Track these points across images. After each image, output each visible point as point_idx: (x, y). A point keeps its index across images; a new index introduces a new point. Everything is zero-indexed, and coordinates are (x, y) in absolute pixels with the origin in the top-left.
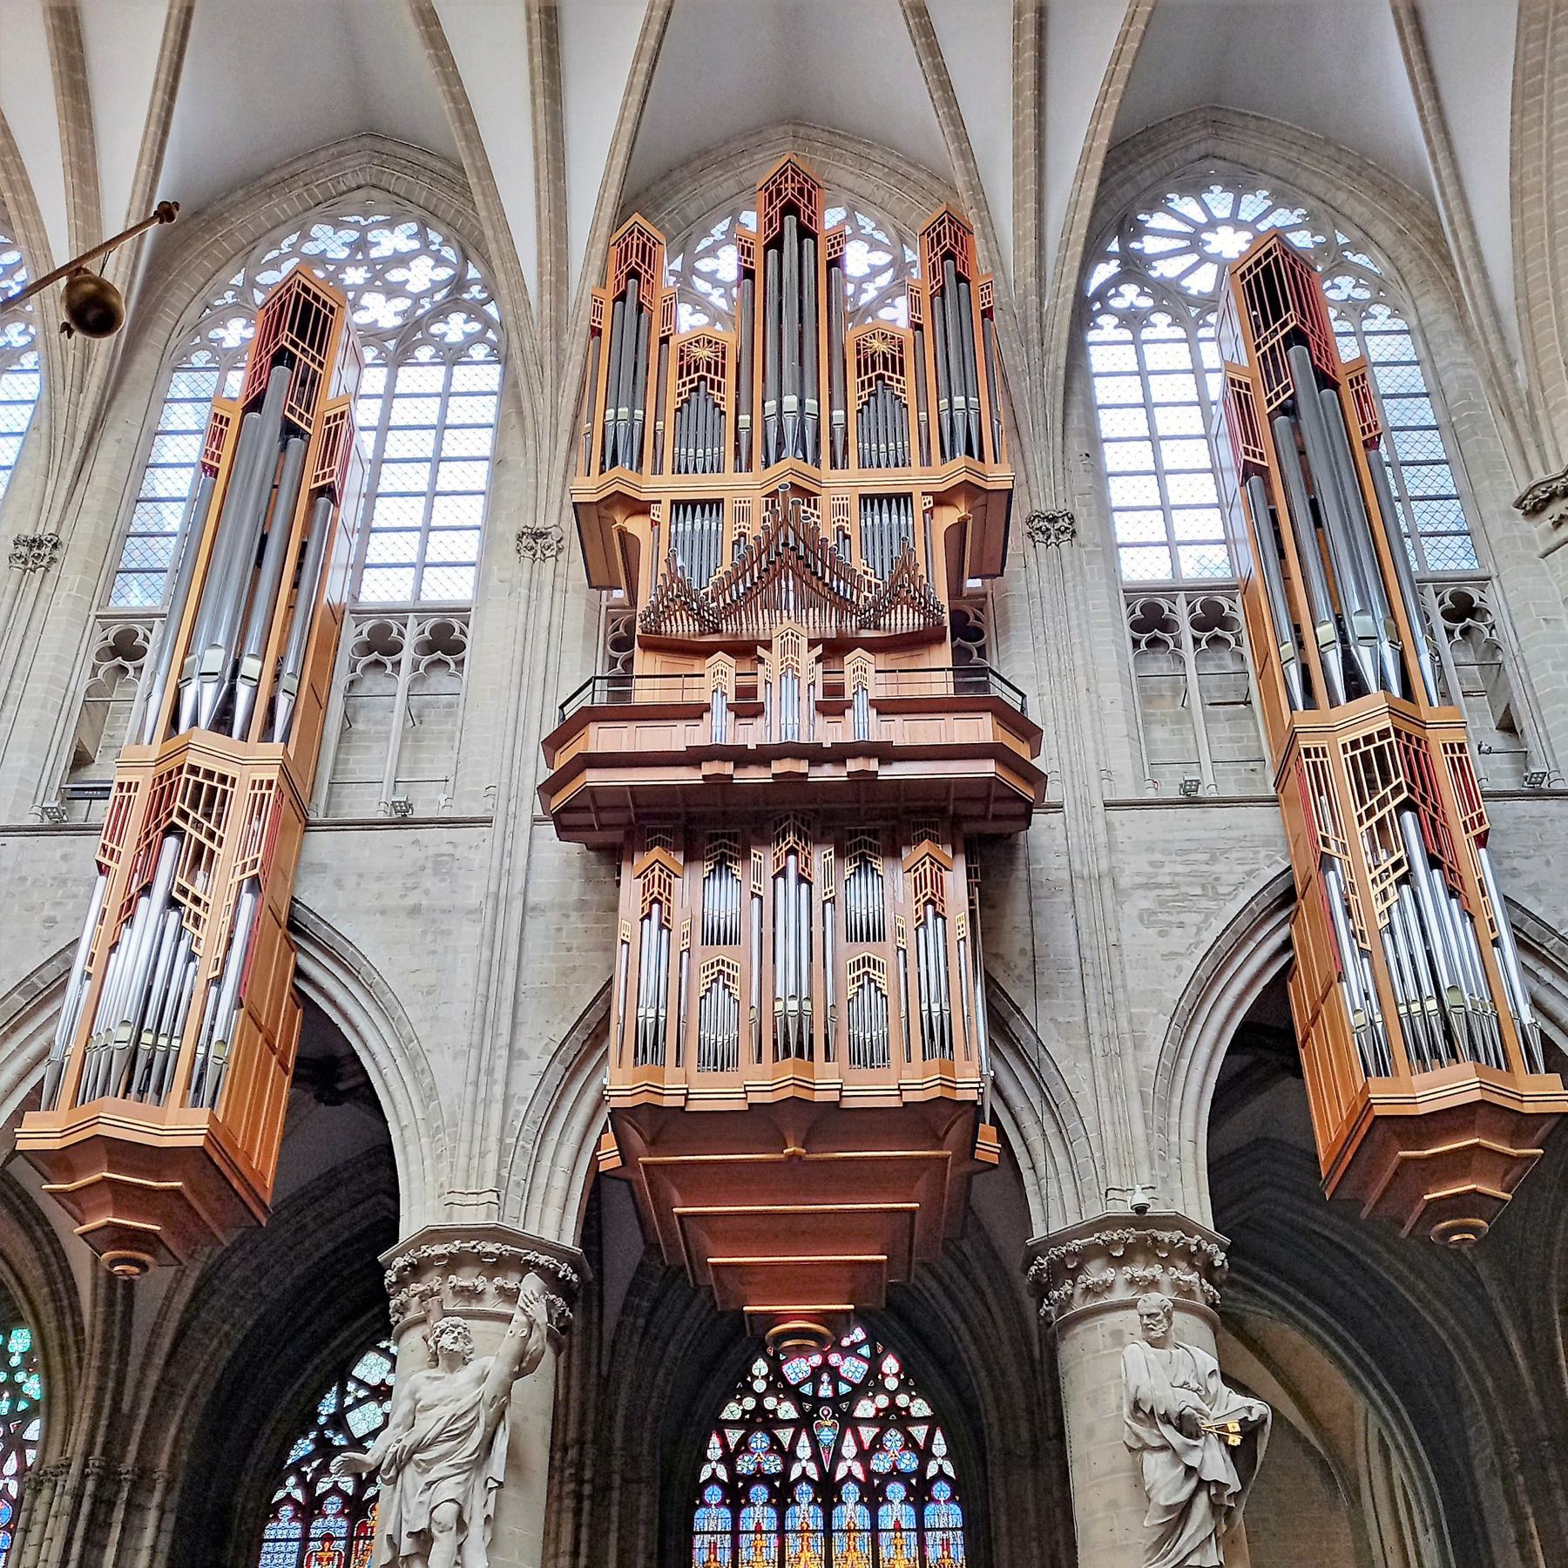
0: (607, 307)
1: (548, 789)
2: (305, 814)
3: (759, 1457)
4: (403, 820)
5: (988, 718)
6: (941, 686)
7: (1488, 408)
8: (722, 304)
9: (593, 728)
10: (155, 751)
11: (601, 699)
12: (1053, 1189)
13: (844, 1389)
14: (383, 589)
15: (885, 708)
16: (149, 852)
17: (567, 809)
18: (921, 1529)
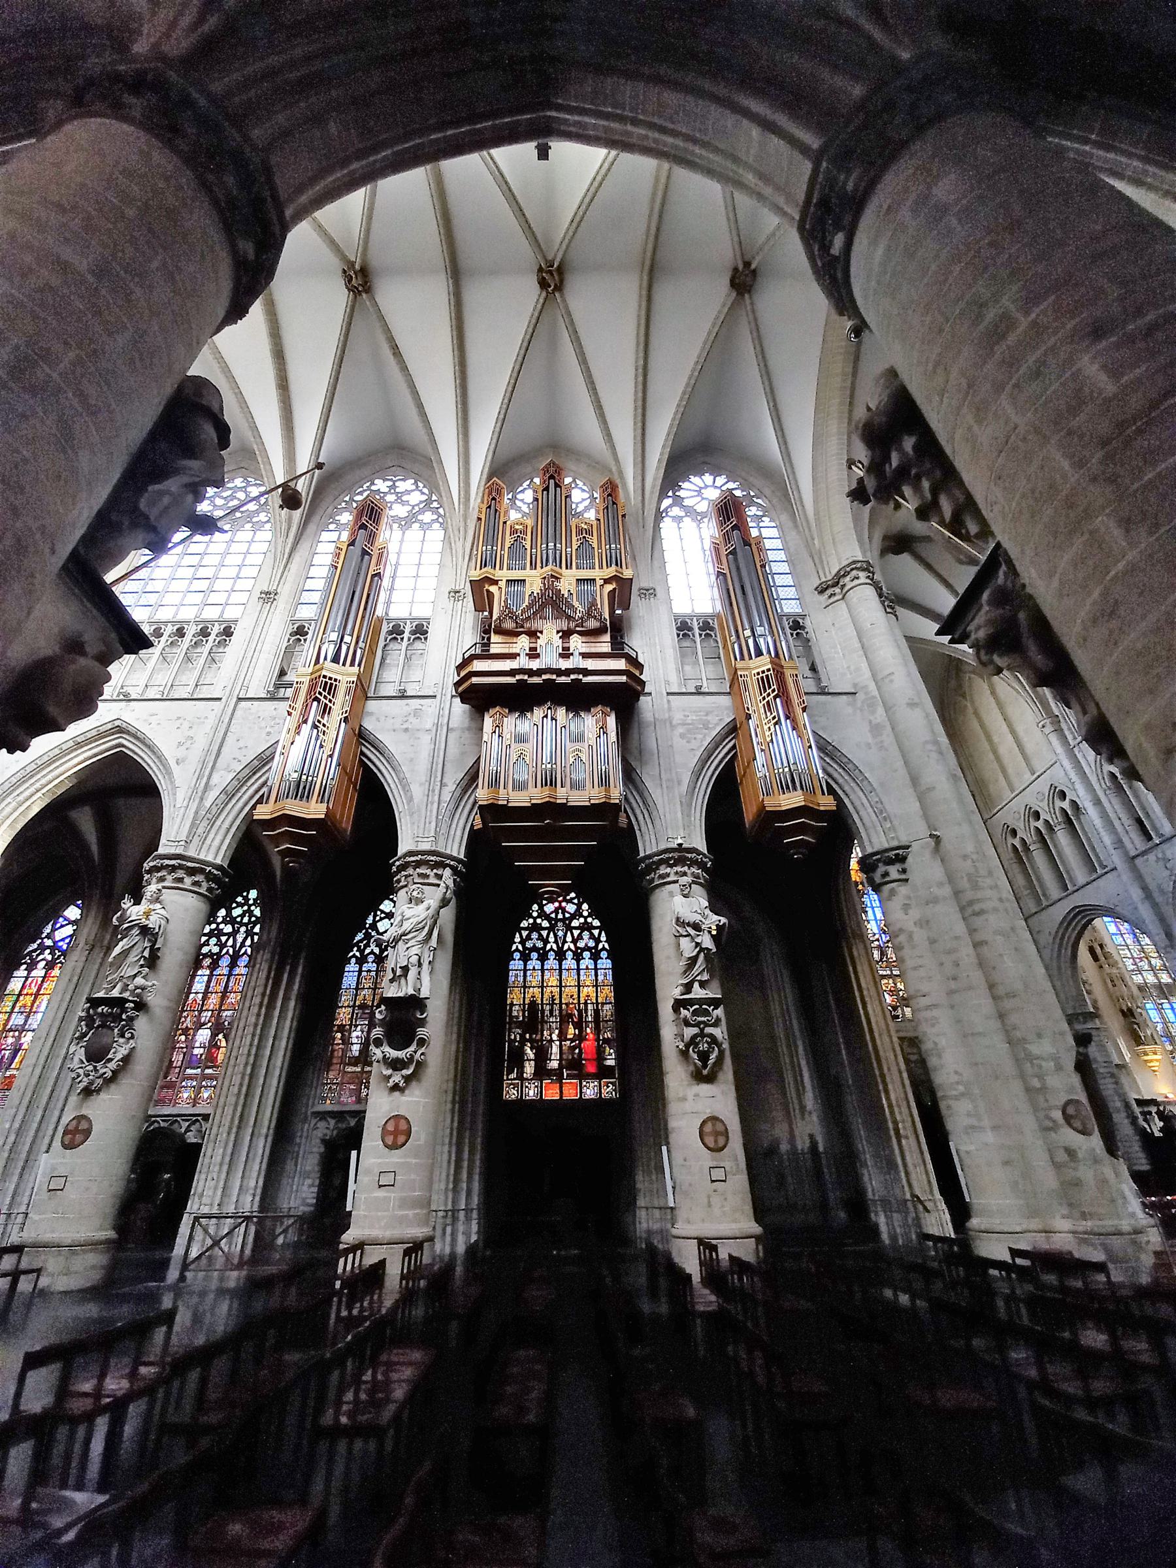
0: (484, 510)
1: (457, 684)
2: (365, 693)
3: (535, 941)
4: (403, 696)
5: (623, 660)
6: (606, 648)
7: (806, 555)
8: (527, 511)
9: (475, 662)
10: (310, 670)
11: (478, 651)
12: (647, 838)
13: (567, 915)
14: (394, 613)
15: (585, 656)
16: (307, 707)
17: (464, 691)
18: (596, 969)
